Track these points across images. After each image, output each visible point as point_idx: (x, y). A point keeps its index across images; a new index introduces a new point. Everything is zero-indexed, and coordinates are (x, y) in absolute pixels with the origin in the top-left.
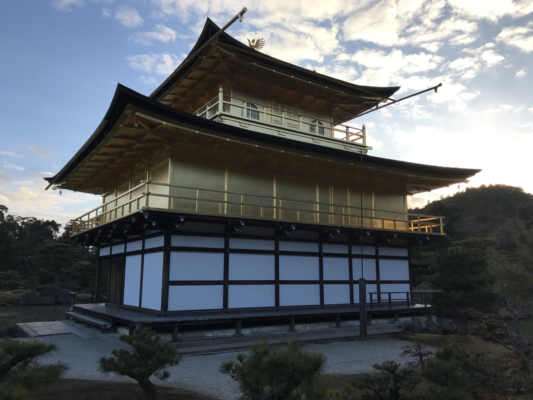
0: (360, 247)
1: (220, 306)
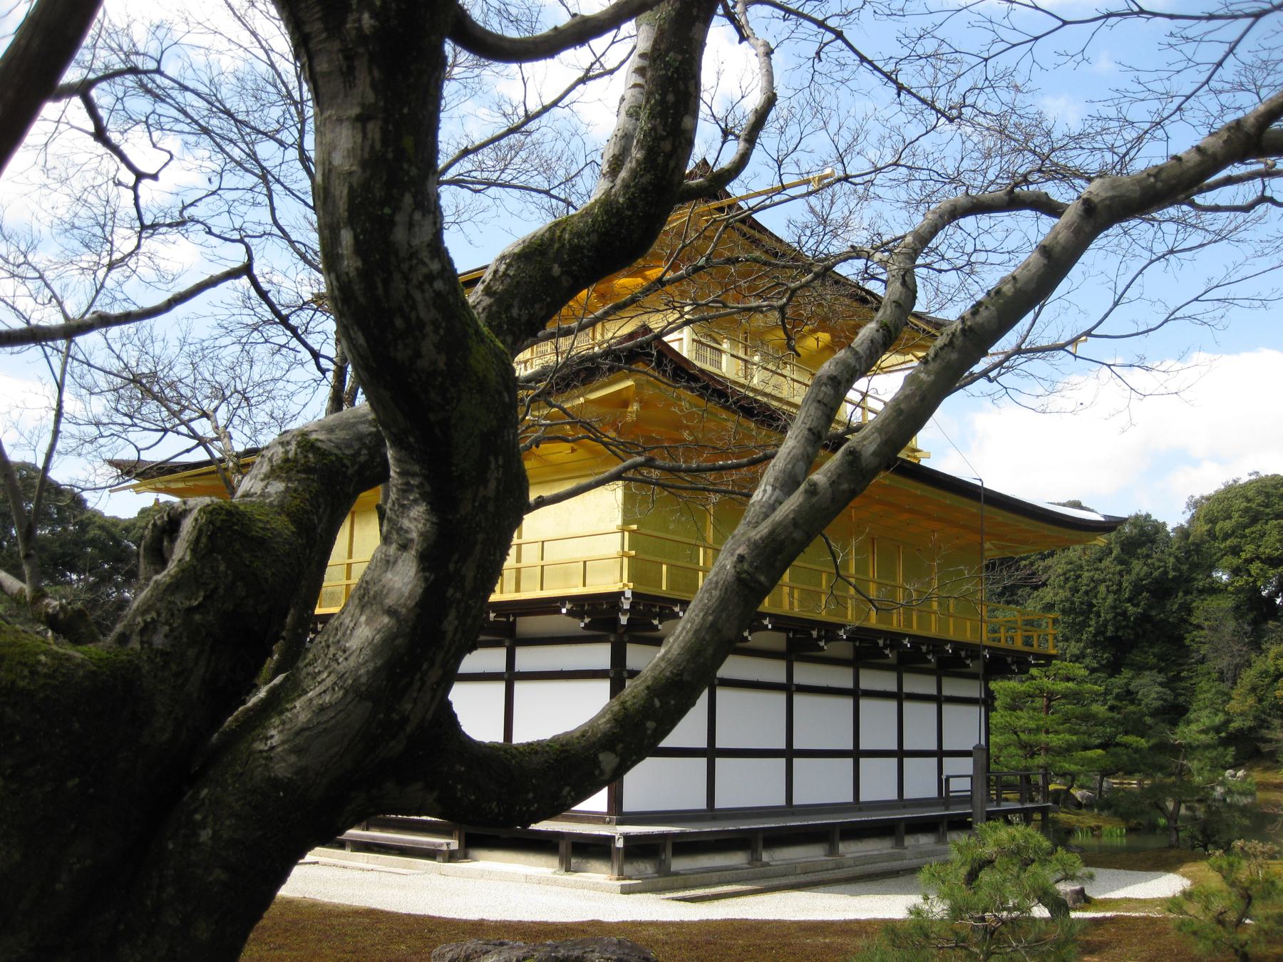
1: (701, 804)
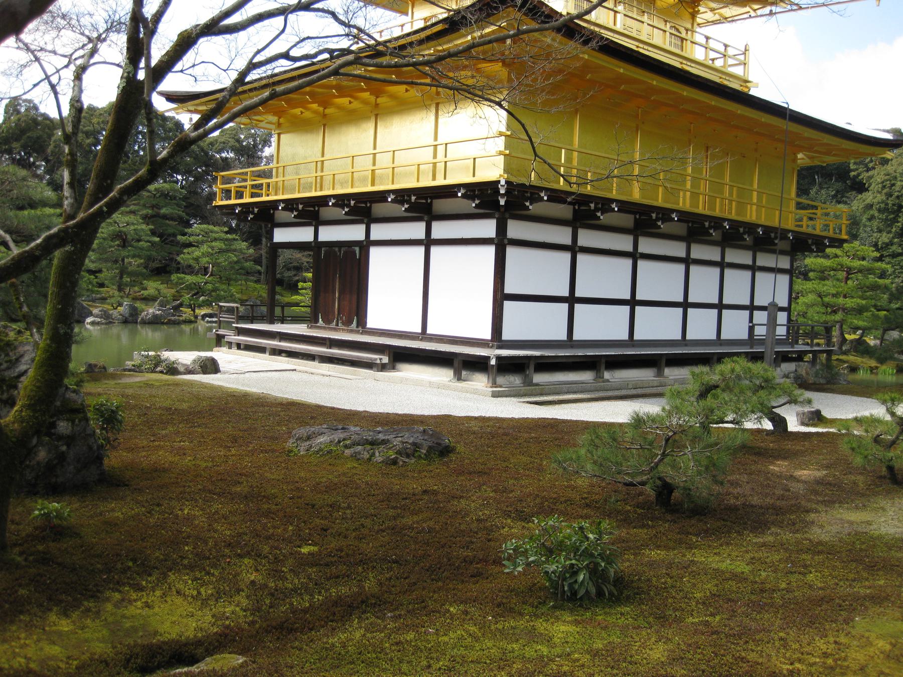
0: (774, 256)
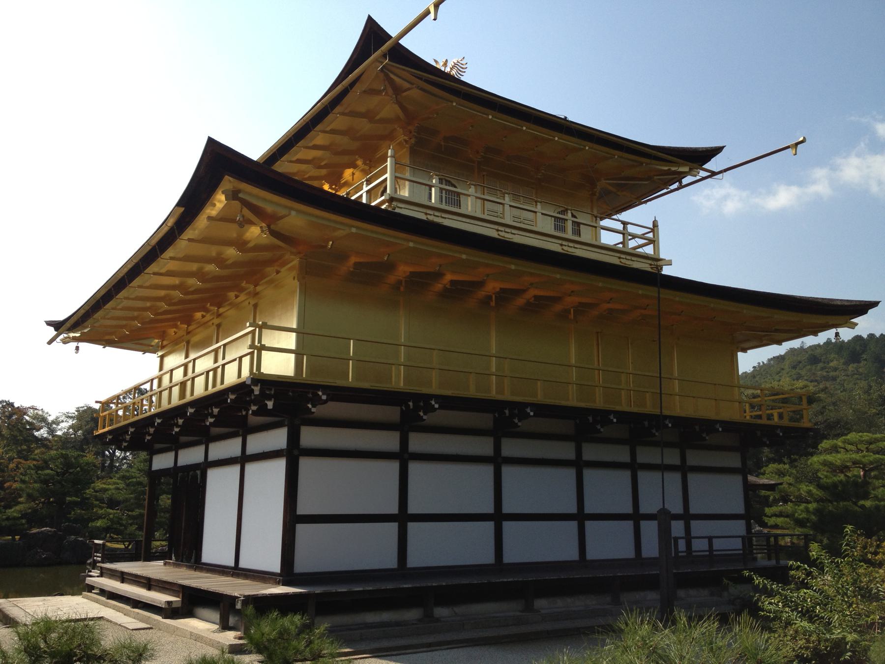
1: (391, 562)
